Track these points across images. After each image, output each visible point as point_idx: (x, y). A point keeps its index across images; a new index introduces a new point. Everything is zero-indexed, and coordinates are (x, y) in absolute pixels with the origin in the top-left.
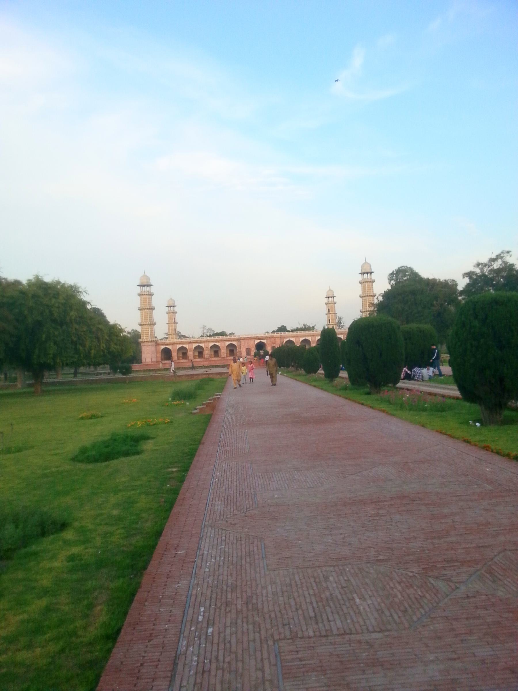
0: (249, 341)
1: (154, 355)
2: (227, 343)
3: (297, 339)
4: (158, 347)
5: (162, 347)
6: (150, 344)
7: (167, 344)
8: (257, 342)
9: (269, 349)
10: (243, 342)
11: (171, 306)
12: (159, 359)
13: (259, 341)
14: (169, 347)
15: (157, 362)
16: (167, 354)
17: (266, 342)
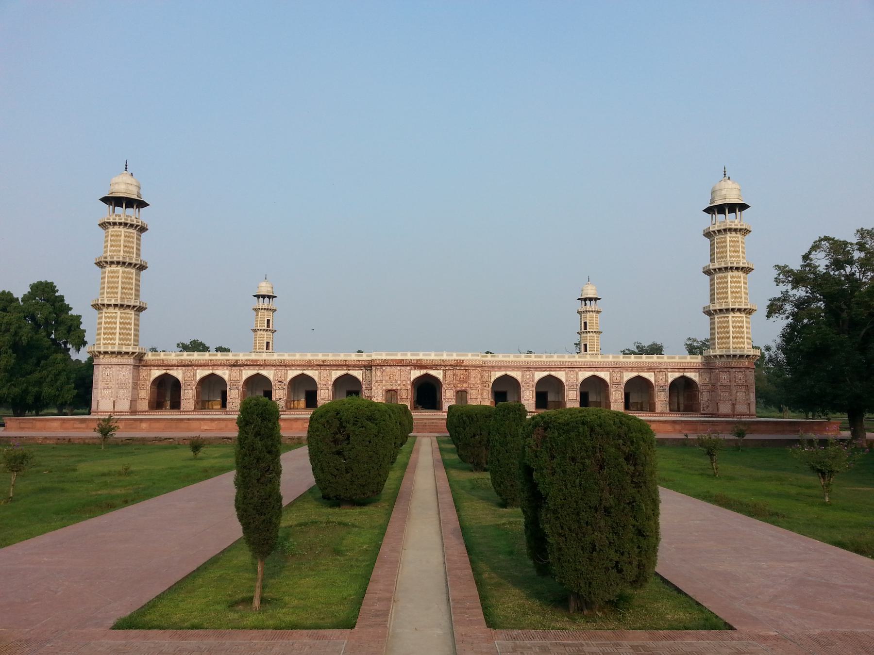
0: (396, 370)
1: (126, 394)
2: (337, 373)
3: (528, 374)
4: (143, 372)
5: (156, 373)
6: (114, 360)
7: (172, 366)
8: (416, 374)
9: (448, 398)
10: (379, 373)
11: (264, 297)
12: (143, 405)
13: (423, 372)
14: (177, 374)
15: (133, 412)
16: (166, 391)
17: (441, 377)
